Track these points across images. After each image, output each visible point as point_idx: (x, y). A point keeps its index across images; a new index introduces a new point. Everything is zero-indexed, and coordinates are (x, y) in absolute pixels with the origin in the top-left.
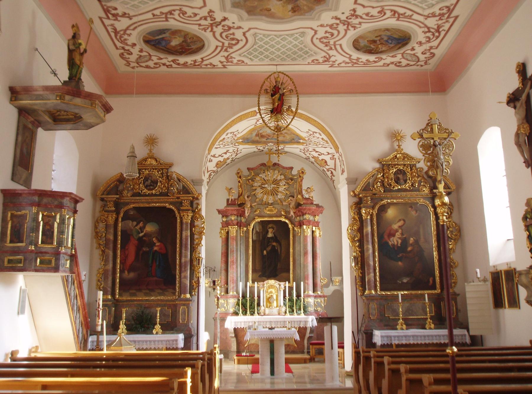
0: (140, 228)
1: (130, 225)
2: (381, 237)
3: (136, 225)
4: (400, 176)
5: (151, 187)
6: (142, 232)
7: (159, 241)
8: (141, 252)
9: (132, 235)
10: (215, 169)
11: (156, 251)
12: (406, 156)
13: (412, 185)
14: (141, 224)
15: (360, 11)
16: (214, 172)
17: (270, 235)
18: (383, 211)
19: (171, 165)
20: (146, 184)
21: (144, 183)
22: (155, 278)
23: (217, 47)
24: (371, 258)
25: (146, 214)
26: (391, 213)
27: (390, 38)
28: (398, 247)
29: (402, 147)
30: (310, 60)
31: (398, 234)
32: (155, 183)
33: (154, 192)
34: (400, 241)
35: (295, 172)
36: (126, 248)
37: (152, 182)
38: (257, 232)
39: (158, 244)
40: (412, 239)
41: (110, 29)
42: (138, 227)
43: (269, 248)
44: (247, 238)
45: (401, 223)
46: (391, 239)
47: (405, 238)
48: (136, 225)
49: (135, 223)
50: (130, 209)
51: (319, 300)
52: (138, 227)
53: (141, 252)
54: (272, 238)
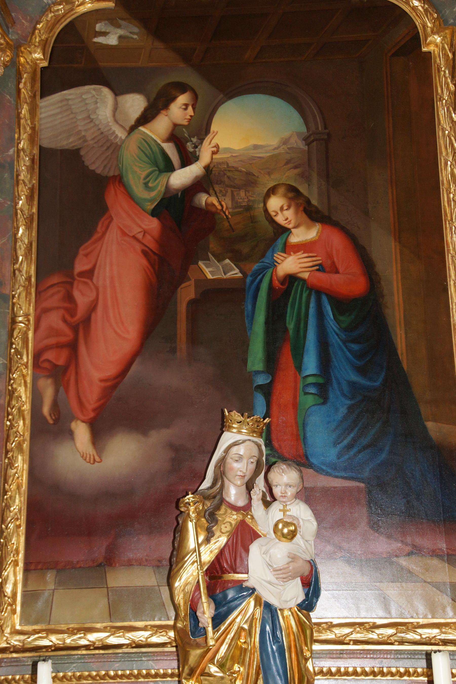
0: (174, 137)
1: (105, 112)
3: (146, 118)
6: (187, 159)
7: (312, 214)
8: (187, 293)
9: (119, 179)
11: (291, 279)
14: (179, 110)
36: (81, 265)
39: (303, 234)
48: (146, 118)
49: (135, 104)
52: (160, 127)
53: (187, 293)
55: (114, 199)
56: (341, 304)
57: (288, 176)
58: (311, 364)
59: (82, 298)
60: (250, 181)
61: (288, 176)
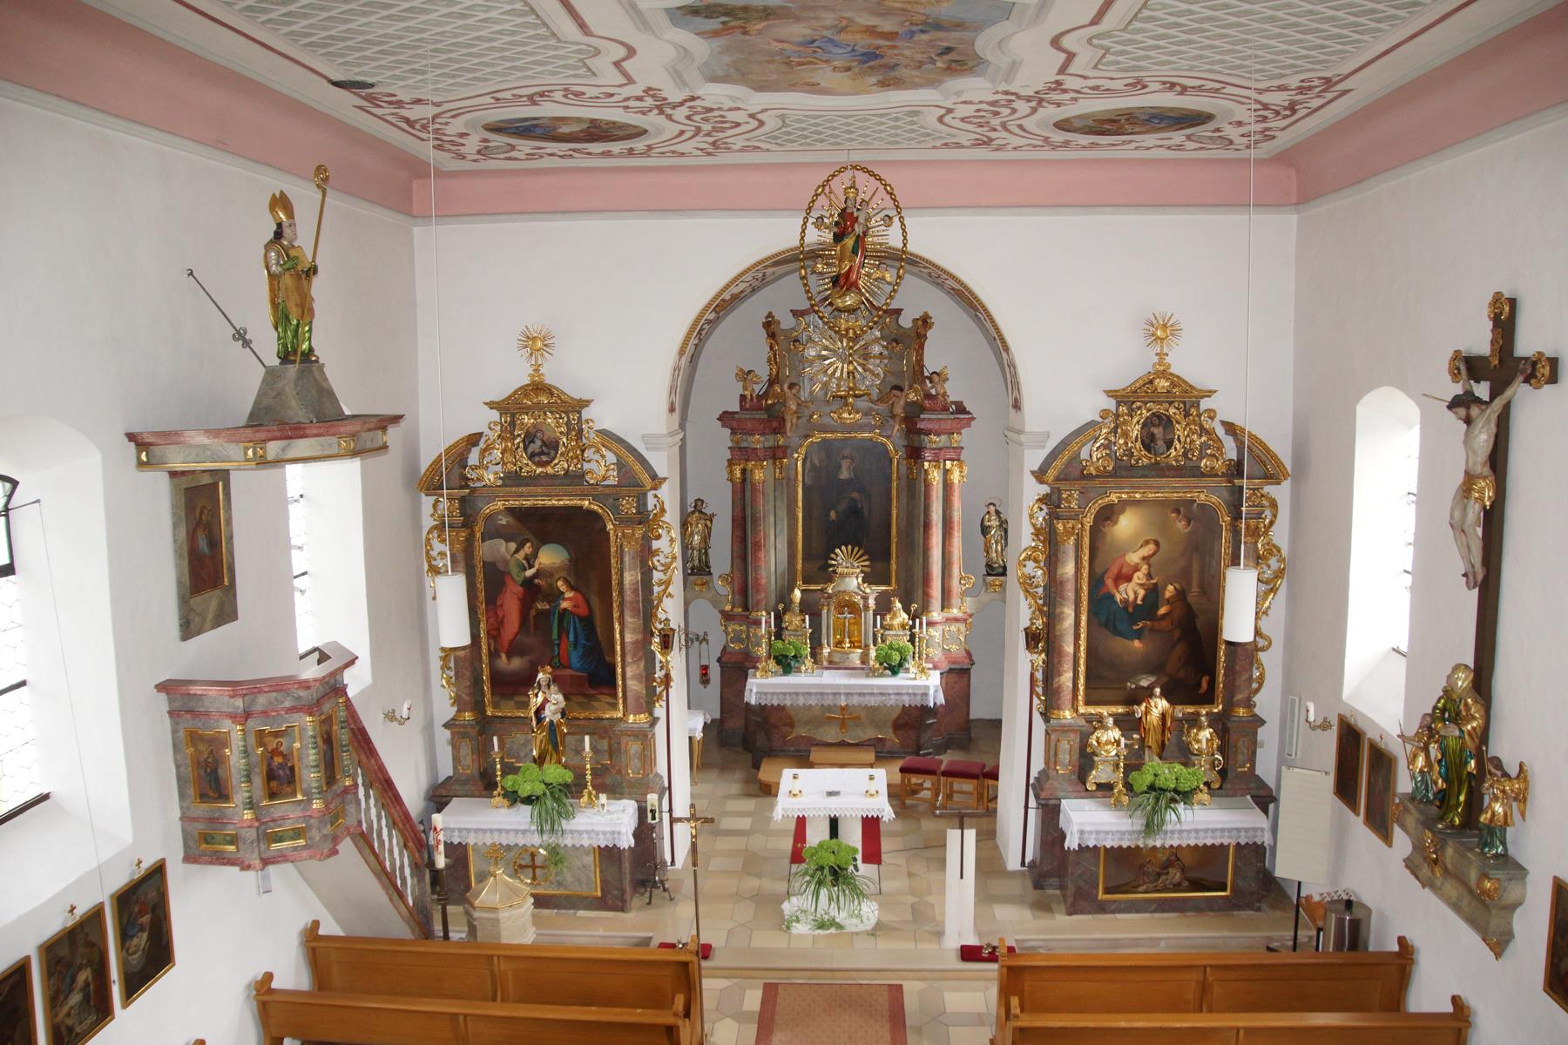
0: (526, 558)
1: (503, 549)
2: (1096, 581)
3: (517, 551)
4: (1158, 432)
5: (544, 458)
6: (531, 567)
7: (572, 588)
8: (533, 613)
10: (712, 316)
12: (1177, 381)
13: (1185, 455)
14: (527, 549)
15: (1070, 83)
16: (709, 322)
17: (844, 474)
18: (1108, 519)
19: (585, 403)
20: (530, 450)
21: (525, 449)
22: (568, 672)
23: (682, 133)
24: (1070, 638)
25: (538, 525)
26: (1127, 525)
27: (1154, 116)
28: (1136, 606)
29: (1168, 360)
30: (938, 143)
31: (1139, 577)
32: (551, 446)
33: (549, 470)
34: (1141, 593)
35: (906, 322)
37: (544, 443)
38: (813, 465)
39: (569, 595)
40: (1170, 588)
41: (389, 118)
42: (520, 556)
43: (843, 506)
44: (790, 483)
45: (1150, 548)
46: (1122, 587)
47: (1155, 585)
48: (517, 551)
49: (513, 546)
50: (499, 512)
51: (953, 628)
52: (520, 556)
53: (533, 613)
54: (849, 481)
55: (507, 580)
56: (581, 619)
57: (563, 574)
58: (571, 637)
59: (500, 613)
60: (551, 575)
61: (563, 574)
